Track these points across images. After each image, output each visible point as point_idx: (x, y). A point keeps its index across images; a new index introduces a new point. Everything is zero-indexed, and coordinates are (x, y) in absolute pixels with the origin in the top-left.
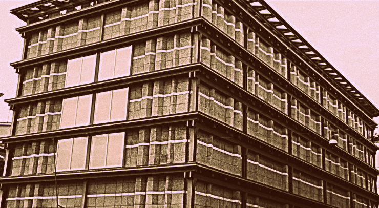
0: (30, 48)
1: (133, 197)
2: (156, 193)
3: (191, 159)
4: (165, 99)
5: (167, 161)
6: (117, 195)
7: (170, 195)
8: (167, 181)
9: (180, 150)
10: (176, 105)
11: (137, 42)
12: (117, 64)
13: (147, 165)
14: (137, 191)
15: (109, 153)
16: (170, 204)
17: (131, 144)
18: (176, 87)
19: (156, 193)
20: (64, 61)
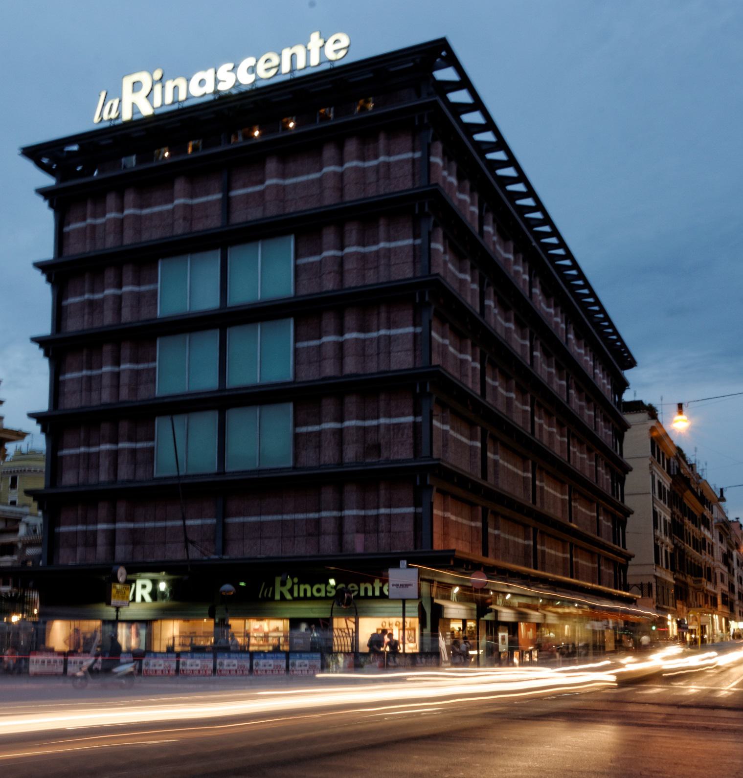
0: (68, 233)
1: (318, 521)
2: (362, 513)
3: (425, 452)
4: (367, 343)
5: (380, 456)
6: (286, 517)
7: (389, 516)
8: (382, 492)
9: (402, 435)
10: (390, 353)
11: (304, 228)
12: (268, 273)
13: (341, 463)
14: (325, 510)
15: (264, 441)
16: (390, 531)
17: (306, 424)
18: (388, 319)
19: (362, 513)
20: (152, 264)
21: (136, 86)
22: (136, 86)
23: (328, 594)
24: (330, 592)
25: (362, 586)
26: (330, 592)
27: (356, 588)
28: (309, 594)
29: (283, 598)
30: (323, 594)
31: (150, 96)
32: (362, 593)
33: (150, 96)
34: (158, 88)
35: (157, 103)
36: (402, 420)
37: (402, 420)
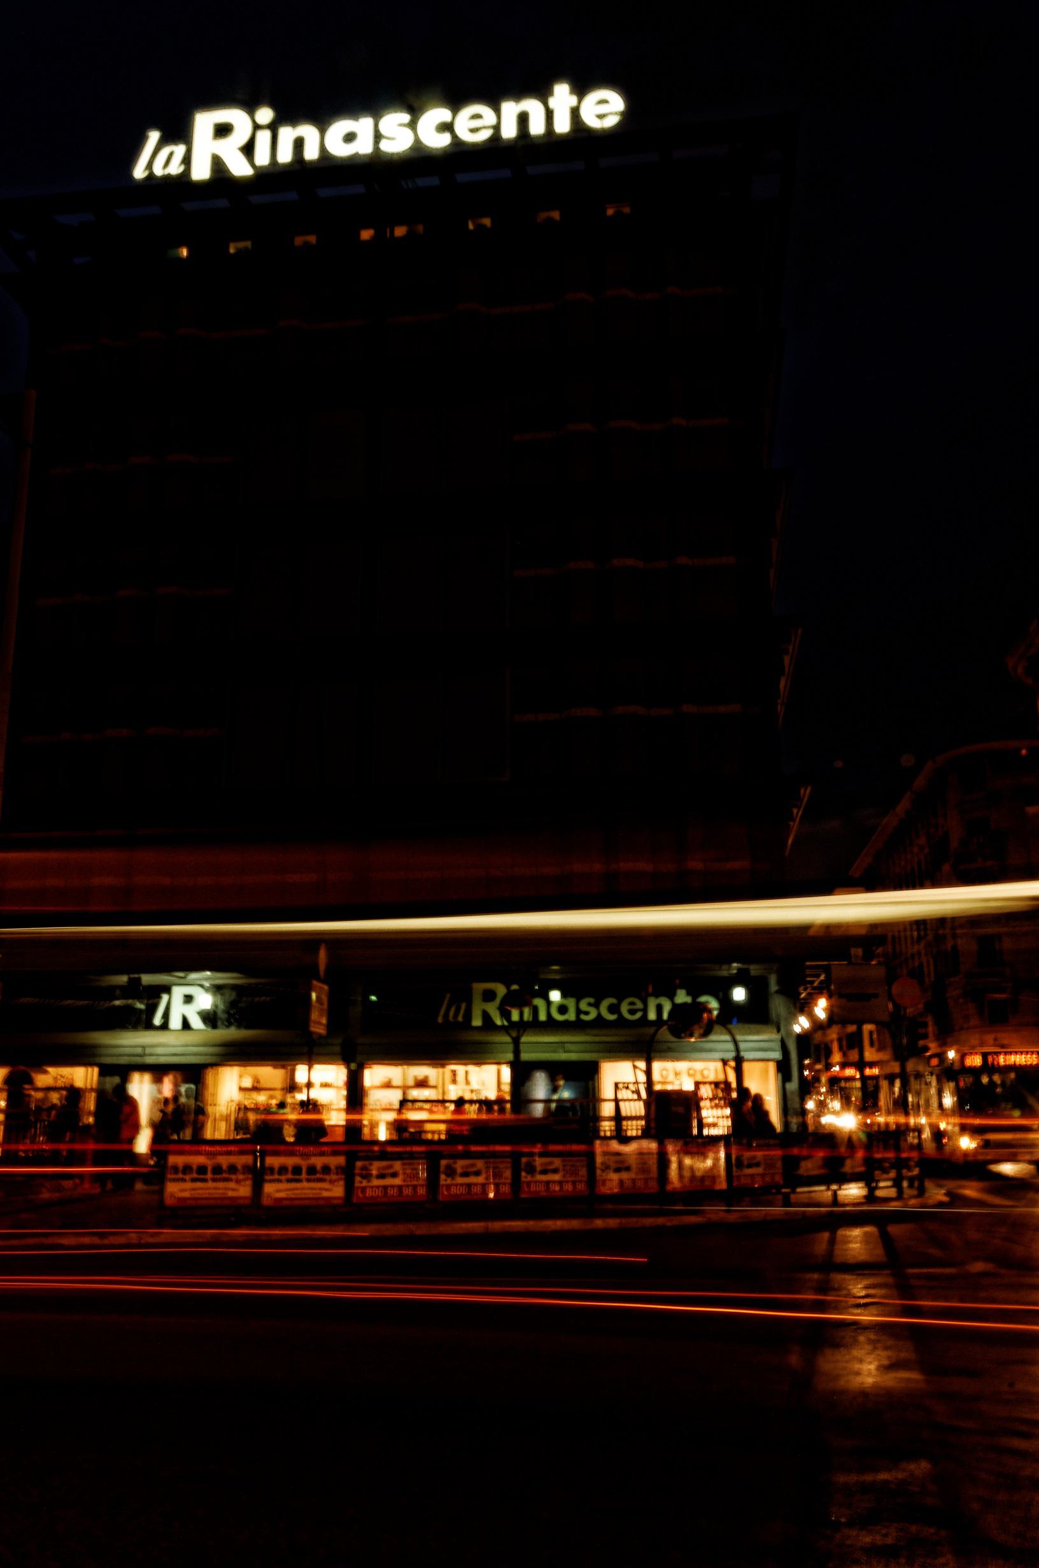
21: (223, 130)
23: (583, 1017)
24: (587, 1013)
25: (652, 1004)
26: (587, 1013)
27: (639, 1005)
28: (543, 1017)
29: (488, 1025)
30: (571, 1016)
31: (248, 150)
32: (652, 1016)
33: (248, 150)
34: (264, 137)
35: (262, 157)
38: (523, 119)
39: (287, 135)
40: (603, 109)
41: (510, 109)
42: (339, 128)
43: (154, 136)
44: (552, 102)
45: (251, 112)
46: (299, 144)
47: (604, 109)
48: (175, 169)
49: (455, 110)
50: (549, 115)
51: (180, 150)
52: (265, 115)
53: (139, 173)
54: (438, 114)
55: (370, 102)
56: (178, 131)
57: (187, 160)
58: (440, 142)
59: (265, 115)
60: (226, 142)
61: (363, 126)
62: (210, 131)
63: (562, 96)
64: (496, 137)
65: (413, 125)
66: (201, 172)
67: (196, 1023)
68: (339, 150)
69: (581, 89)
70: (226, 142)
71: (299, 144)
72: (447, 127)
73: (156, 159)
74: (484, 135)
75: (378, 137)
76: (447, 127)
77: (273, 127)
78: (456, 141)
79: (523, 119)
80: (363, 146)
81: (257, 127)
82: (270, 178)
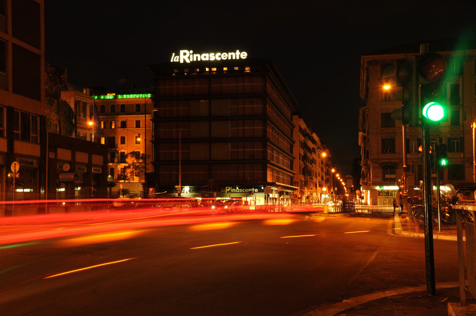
21: (185, 54)
22: (185, 54)
31: (189, 58)
34: (191, 56)
35: (191, 60)
36: (260, 150)
37: (260, 150)
38: (232, 56)
39: (195, 55)
40: (244, 55)
41: (230, 54)
42: (204, 55)
43: (174, 54)
44: (236, 53)
45: (189, 51)
46: (197, 57)
47: (244, 55)
48: (177, 61)
49: (222, 53)
50: (236, 55)
51: (178, 57)
52: (191, 52)
53: (172, 61)
54: (219, 54)
55: (208, 51)
56: (177, 54)
57: (179, 59)
58: (219, 59)
59: (191, 52)
60: (185, 56)
61: (207, 55)
62: (183, 54)
63: (238, 51)
64: (228, 58)
65: (215, 55)
66: (182, 61)
67: (188, 192)
68: (204, 59)
69: (241, 51)
70: (185, 56)
71: (197, 57)
72: (220, 56)
73: (174, 59)
74: (226, 58)
75: (209, 58)
76: (220, 56)
77: (193, 54)
78: (221, 59)
79: (232, 56)
80: (207, 59)
81: (190, 54)
82: (193, 63)
